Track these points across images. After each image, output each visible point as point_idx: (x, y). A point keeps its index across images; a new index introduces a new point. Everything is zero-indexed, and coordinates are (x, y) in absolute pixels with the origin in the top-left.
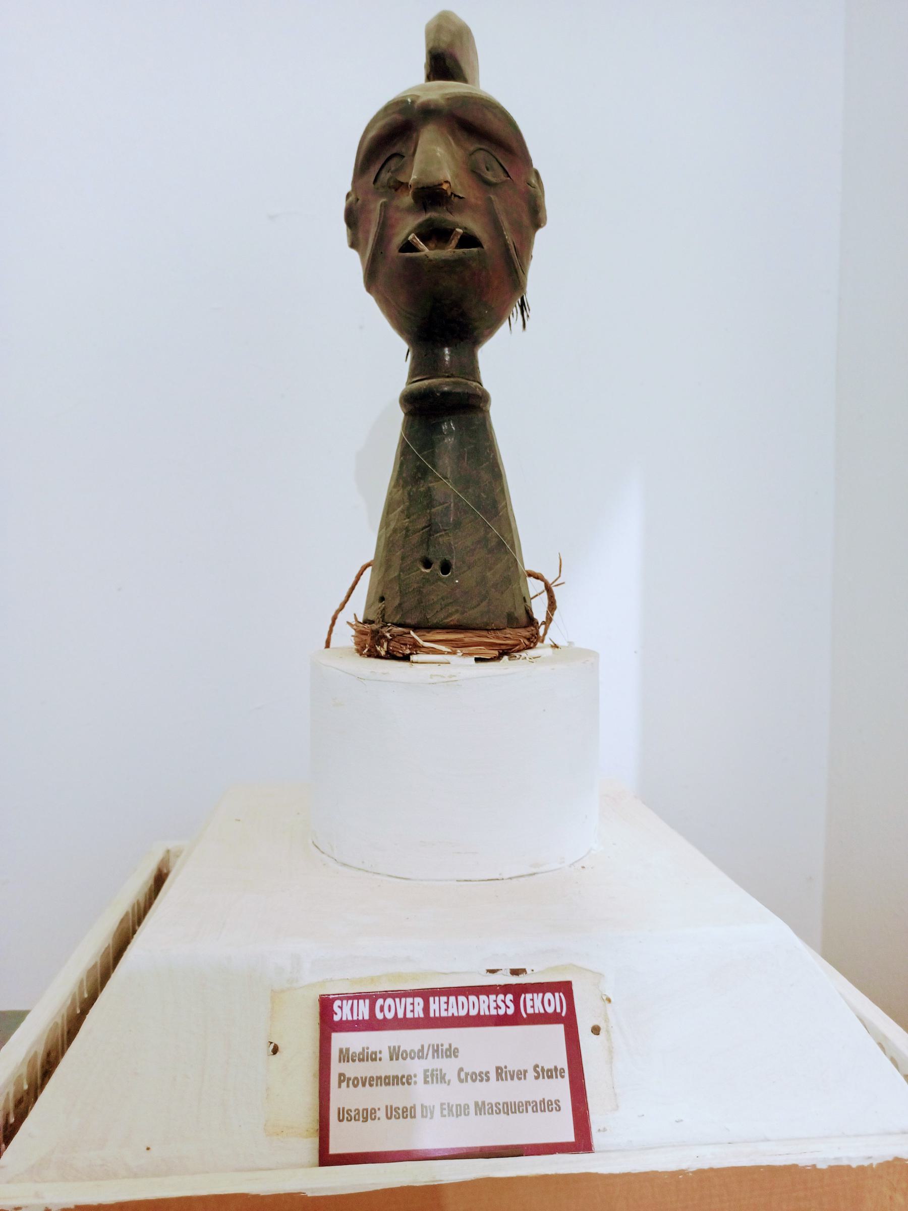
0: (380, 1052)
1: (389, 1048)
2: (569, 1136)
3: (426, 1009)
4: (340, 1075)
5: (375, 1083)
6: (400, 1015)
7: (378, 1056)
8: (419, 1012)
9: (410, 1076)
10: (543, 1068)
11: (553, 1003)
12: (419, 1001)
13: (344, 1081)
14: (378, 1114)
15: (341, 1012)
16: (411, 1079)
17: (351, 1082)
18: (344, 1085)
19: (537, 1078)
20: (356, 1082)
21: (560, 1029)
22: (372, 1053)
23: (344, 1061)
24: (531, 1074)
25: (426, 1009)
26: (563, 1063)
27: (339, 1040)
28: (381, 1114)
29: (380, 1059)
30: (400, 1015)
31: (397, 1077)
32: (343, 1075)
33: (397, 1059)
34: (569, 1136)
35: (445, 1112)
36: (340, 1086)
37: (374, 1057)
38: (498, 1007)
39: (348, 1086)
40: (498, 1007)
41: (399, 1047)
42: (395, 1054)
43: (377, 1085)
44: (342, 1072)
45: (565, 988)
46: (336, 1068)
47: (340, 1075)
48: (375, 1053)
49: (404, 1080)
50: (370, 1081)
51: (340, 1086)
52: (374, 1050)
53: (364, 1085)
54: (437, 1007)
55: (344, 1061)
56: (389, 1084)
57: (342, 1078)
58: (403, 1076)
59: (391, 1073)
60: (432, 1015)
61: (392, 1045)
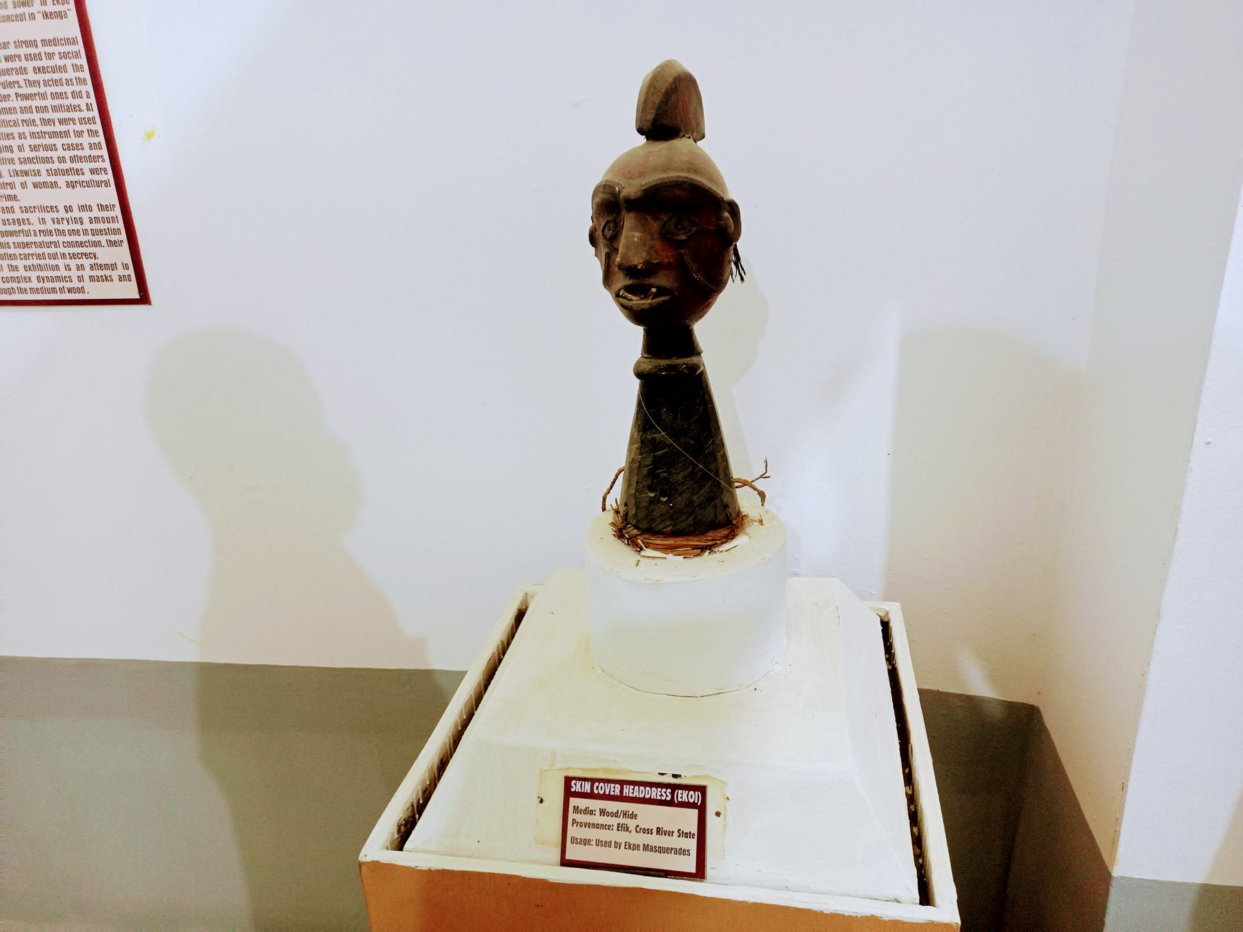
2: (692, 869)
3: (621, 791)
4: (573, 820)
6: (607, 793)
8: (617, 792)
10: (683, 832)
11: (694, 797)
12: (618, 786)
14: (592, 843)
15: (576, 786)
18: (575, 825)
19: (679, 836)
20: (581, 825)
21: (695, 812)
24: (676, 834)
25: (621, 791)
26: (695, 830)
27: (574, 801)
28: (593, 843)
30: (607, 793)
34: (692, 869)
35: (627, 847)
36: (573, 825)
37: (592, 813)
38: (661, 795)
40: (661, 795)
42: (603, 812)
45: (702, 790)
46: (571, 816)
47: (573, 820)
51: (573, 825)
53: (585, 827)
54: (628, 791)
59: (601, 823)
60: (624, 795)
61: (602, 808)
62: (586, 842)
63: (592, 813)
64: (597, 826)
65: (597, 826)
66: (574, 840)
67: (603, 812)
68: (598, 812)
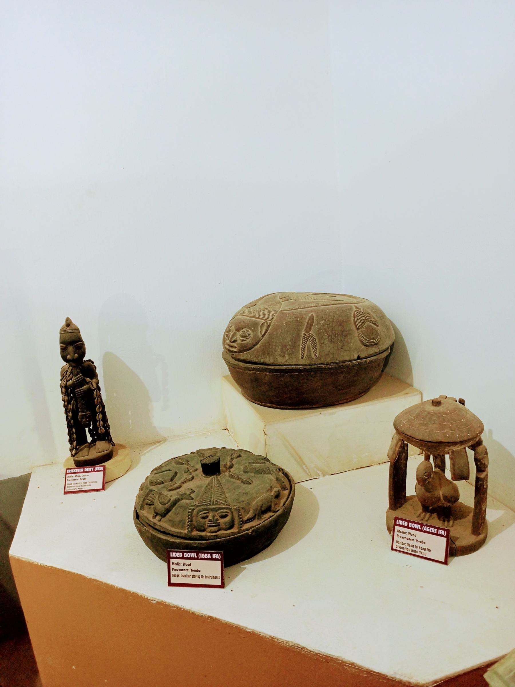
2: (220, 583)
7: (181, 564)
18: (173, 570)
20: (176, 570)
21: (220, 562)
34: (220, 583)
37: (180, 565)
44: (173, 567)
47: (173, 568)
53: (178, 570)
56: (183, 571)
57: (173, 569)
62: (177, 576)
63: (180, 565)
64: (183, 570)
65: (183, 570)
66: (174, 576)
67: (184, 564)
68: (182, 564)
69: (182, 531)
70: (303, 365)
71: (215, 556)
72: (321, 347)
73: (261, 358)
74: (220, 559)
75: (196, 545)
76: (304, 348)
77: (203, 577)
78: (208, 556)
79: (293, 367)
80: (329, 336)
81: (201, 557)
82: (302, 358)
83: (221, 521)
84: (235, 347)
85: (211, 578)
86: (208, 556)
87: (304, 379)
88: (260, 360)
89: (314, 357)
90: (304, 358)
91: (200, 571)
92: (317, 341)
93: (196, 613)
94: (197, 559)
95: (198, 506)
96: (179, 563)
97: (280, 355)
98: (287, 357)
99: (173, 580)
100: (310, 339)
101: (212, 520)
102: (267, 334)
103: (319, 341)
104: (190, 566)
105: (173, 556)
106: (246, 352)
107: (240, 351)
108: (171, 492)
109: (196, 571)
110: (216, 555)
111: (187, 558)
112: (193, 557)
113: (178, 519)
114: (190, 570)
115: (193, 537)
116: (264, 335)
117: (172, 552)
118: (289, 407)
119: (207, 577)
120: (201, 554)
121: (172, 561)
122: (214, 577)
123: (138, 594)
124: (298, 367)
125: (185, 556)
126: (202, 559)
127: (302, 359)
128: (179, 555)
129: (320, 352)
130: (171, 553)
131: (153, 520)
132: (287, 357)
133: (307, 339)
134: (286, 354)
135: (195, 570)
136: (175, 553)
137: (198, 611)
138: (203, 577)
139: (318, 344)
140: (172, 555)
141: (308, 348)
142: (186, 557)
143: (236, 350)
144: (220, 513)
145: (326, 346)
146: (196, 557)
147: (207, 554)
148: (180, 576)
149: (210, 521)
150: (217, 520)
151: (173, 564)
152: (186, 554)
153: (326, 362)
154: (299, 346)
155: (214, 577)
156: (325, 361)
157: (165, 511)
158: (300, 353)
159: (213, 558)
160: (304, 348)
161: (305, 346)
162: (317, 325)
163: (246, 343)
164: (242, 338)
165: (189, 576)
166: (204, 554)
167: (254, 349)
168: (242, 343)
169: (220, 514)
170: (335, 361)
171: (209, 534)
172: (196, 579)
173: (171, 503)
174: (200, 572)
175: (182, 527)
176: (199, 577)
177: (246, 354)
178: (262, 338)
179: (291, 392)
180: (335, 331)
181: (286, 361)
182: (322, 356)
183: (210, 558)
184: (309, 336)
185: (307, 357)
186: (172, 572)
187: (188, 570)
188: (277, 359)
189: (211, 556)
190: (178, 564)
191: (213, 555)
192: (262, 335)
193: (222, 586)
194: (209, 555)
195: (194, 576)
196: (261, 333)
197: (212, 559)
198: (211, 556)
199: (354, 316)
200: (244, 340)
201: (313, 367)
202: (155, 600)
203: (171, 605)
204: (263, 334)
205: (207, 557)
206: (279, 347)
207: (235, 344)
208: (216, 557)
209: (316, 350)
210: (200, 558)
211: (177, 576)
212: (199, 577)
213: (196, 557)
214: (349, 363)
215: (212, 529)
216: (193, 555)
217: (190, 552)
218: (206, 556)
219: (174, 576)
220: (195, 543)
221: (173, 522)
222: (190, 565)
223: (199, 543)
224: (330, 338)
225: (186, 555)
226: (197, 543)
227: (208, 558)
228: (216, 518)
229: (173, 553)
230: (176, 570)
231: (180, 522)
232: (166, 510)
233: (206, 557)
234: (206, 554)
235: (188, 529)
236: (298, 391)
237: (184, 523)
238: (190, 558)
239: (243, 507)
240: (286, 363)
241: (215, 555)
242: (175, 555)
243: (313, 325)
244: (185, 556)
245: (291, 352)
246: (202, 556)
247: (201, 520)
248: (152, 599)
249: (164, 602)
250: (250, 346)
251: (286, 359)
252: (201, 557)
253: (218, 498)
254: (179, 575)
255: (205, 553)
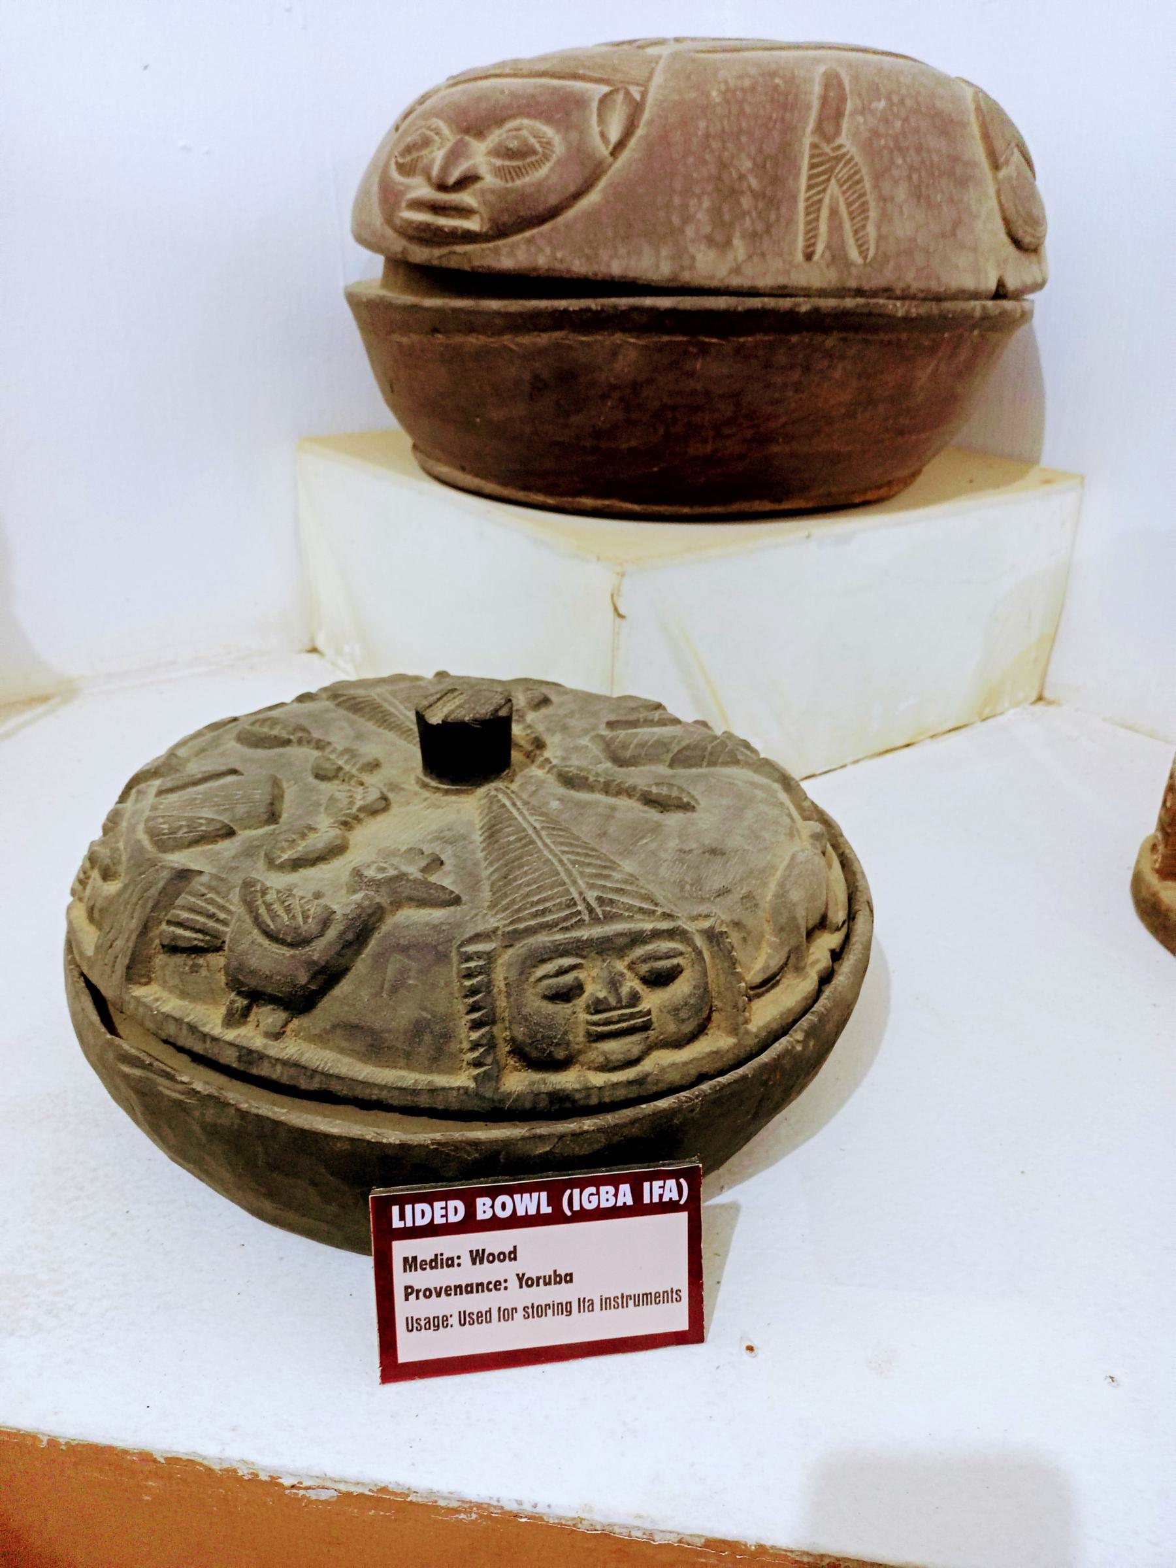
0: (459, 1257)
1: (471, 1252)
2: (683, 1325)
4: (406, 1288)
5: (453, 1292)
7: (456, 1261)
9: (500, 1282)
13: (411, 1293)
16: (500, 1284)
17: (421, 1294)
18: (413, 1297)
20: (428, 1293)
21: (684, 1216)
22: (448, 1259)
23: (411, 1271)
29: (459, 1265)
31: (482, 1284)
32: (411, 1287)
33: (481, 1262)
34: (683, 1325)
36: (407, 1299)
37: (450, 1263)
39: (418, 1298)
41: (484, 1251)
42: (478, 1257)
43: (456, 1294)
47: (406, 1288)
48: (452, 1259)
49: (491, 1286)
50: (446, 1291)
51: (407, 1299)
52: (450, 1256)
53: (439, 1295)
55: (411, 1271)
56: (472, 1292)
57: (409, 1291)
58: (489, 1283)
59: (475, 1281)
63: (450, 1263)
64: (469, 1289)
65: (469, 1289)
66: (413, 1325)
67: (478, 1257)
68: (466, 1260)
69: (441, 1080)
70: (807, 293)
71: (657, 1192)
72: (884, 216)
73: (611, 257)
74: (682, 1202)
75: (548, 1149)
76: (814, 207)
77: (586, 1305)
78: (616, 1195)
79: (766, 300)
80: (912, 168)
81: (576, 1207)
82: (809, 257)
83: (653, 1000)
84: (463, 212)
85: (631, 1303)
86: (616, 1195)
87: (792, 367)
88: (608, 266)
89: (854, 254)
90: (816, 257)
91: (569, 1278)
92: (867, 185)
93: (617, 1530)
94: (557, 1218)
95: (513, 937)
96: (445, 1257)
97: (710, 241)
98: (740, 247)
99: (409, 1349)
100: (842, 171)
101: (613, 1002)
102: (633, 142)
103: (876, 186)
104: (515, 1259)
105: (409, 1224)
106: (528, 234)
107: (499, 231)
108: (303, 872)
109: (545, 1284)
110: (663, 1187)
111: (495, 1224)
112: (532, 1211)
113: (405, 1013)
114: (514, 1283)
115: (515, 1101)
116: (621, 145)
117: (402, 1201)
118: (686, 510)
119: (606, 1303)
120: (576, 1192)
121: (401, 1249)
122: (645, 1299)
123: (206, 1463)
124: (785, 304)
125: (480, 1216)
126: (583, 1216)
127: (805, 265)
128: (443, 1212)
129: (880, 238)
130: (395, 1210)
131: (230, 1035)
132: (740, 247)
133: (830, 170)
134: (738, 234)
135: (538, 1278)
136: (419, 1207)
137: (637, 1523)
138: (586, 1305)
139: (871, 198)
140: (402, 1217)
141: (834, 212)
142: (489, 1215)
143: (472, 224)
144: (645, 959)
145: (901, 213)
146: (546, 1209)
147: (611, 1189)
148: (454, 1320)
149: (598, 1006)
150: (635, 998)
151: (411, 1264)
152: (488, 1201)
153: (901, 285)
154: (794, 198)
155: (645, 1299)
156: (899, 279)
157: (313, 978)
158: (796, 235)
159: (647, 1200)
160: (814, 207)
161: (820, 201)
162: (862, 113)
163: (532, 185)
164: (507, 163)
165: (507, 1314)
166: (593, 1190)
167: (570, 214)
168: (510, 185)
169: (644, 968)
170: (933, 285)
171: (598, 1079)
172: (550, 1319)
173: (342, 934)
174: (571, 1281)
175: (439, 1058)
176: (565, 1309)
177: (530, 241)
178: (610, 159)
179: (726, 431)
180: (929, 150)
181: (737, 270)
182: (886, 258)
183: (630, 1202)
184: (838, 159)
185: (828, 254)
186: (403, 1309)
187: (497, 1284)
188: (693, 258)
189: (637, 1193)
190: (435, 1263)
191: (646, 1185)
192: (611, 147)
193: (694, 1334)
194: (625, 1188)
195: (536, 1311)
196: (603, 135)
197: (638, 1208)
198: (637, 1193)
199: (978, 109)
200: (519, 172)
201: (849, 303)
202: (328, 1484)
203: (442, 1503)
204: (614, 135)
205: (611, 1204)
206: (700, 203)
207: (466, 198)
208: (661, 1196)
209: (864, 227)
210: (569, 1213)
211: (438, 1323)
212: (565, 1309)
213: (546, 1209)
214: (975, 306)
215: (614, 1048)
216: (529, 1203)
217: (510, 1191)
218: (606, 1197)
219: (413, 1325)
220: (541, 1137)
221: (371, 1032)
222: (513, 1255)
223: (561, 1137)
224: (915, 177)
225: (484, 1208)
226: (550, 1136)
227: (620, 1204)
228: (625, 990)
229: (408, 1208)
230: (428, 1293)
231: (418, 1029)
232: (318, 973)
233: (604, 1205)
234: (603, 1189)
235: (477, 1064)
236: (754, 426)
237: (447, 1036)
238: (515, 1222)
239: (736, 917)
240: (735, 282)
241: (657, 1184)
242: (420, 1214)
243: (847, 113)
244: (480, 1216)
245: (760, 227)
246: (585, 1199)
247: (550, 1008)
248: (306, 1484)
249: (394, 1493)
250: (553, 200)
251: (735, 259)
252: (576, 1207)
253: (604, 886)
254: (445, 1318)
255: (598, 1183)
